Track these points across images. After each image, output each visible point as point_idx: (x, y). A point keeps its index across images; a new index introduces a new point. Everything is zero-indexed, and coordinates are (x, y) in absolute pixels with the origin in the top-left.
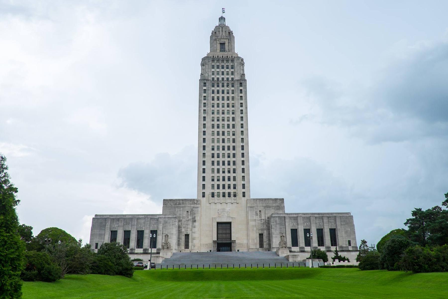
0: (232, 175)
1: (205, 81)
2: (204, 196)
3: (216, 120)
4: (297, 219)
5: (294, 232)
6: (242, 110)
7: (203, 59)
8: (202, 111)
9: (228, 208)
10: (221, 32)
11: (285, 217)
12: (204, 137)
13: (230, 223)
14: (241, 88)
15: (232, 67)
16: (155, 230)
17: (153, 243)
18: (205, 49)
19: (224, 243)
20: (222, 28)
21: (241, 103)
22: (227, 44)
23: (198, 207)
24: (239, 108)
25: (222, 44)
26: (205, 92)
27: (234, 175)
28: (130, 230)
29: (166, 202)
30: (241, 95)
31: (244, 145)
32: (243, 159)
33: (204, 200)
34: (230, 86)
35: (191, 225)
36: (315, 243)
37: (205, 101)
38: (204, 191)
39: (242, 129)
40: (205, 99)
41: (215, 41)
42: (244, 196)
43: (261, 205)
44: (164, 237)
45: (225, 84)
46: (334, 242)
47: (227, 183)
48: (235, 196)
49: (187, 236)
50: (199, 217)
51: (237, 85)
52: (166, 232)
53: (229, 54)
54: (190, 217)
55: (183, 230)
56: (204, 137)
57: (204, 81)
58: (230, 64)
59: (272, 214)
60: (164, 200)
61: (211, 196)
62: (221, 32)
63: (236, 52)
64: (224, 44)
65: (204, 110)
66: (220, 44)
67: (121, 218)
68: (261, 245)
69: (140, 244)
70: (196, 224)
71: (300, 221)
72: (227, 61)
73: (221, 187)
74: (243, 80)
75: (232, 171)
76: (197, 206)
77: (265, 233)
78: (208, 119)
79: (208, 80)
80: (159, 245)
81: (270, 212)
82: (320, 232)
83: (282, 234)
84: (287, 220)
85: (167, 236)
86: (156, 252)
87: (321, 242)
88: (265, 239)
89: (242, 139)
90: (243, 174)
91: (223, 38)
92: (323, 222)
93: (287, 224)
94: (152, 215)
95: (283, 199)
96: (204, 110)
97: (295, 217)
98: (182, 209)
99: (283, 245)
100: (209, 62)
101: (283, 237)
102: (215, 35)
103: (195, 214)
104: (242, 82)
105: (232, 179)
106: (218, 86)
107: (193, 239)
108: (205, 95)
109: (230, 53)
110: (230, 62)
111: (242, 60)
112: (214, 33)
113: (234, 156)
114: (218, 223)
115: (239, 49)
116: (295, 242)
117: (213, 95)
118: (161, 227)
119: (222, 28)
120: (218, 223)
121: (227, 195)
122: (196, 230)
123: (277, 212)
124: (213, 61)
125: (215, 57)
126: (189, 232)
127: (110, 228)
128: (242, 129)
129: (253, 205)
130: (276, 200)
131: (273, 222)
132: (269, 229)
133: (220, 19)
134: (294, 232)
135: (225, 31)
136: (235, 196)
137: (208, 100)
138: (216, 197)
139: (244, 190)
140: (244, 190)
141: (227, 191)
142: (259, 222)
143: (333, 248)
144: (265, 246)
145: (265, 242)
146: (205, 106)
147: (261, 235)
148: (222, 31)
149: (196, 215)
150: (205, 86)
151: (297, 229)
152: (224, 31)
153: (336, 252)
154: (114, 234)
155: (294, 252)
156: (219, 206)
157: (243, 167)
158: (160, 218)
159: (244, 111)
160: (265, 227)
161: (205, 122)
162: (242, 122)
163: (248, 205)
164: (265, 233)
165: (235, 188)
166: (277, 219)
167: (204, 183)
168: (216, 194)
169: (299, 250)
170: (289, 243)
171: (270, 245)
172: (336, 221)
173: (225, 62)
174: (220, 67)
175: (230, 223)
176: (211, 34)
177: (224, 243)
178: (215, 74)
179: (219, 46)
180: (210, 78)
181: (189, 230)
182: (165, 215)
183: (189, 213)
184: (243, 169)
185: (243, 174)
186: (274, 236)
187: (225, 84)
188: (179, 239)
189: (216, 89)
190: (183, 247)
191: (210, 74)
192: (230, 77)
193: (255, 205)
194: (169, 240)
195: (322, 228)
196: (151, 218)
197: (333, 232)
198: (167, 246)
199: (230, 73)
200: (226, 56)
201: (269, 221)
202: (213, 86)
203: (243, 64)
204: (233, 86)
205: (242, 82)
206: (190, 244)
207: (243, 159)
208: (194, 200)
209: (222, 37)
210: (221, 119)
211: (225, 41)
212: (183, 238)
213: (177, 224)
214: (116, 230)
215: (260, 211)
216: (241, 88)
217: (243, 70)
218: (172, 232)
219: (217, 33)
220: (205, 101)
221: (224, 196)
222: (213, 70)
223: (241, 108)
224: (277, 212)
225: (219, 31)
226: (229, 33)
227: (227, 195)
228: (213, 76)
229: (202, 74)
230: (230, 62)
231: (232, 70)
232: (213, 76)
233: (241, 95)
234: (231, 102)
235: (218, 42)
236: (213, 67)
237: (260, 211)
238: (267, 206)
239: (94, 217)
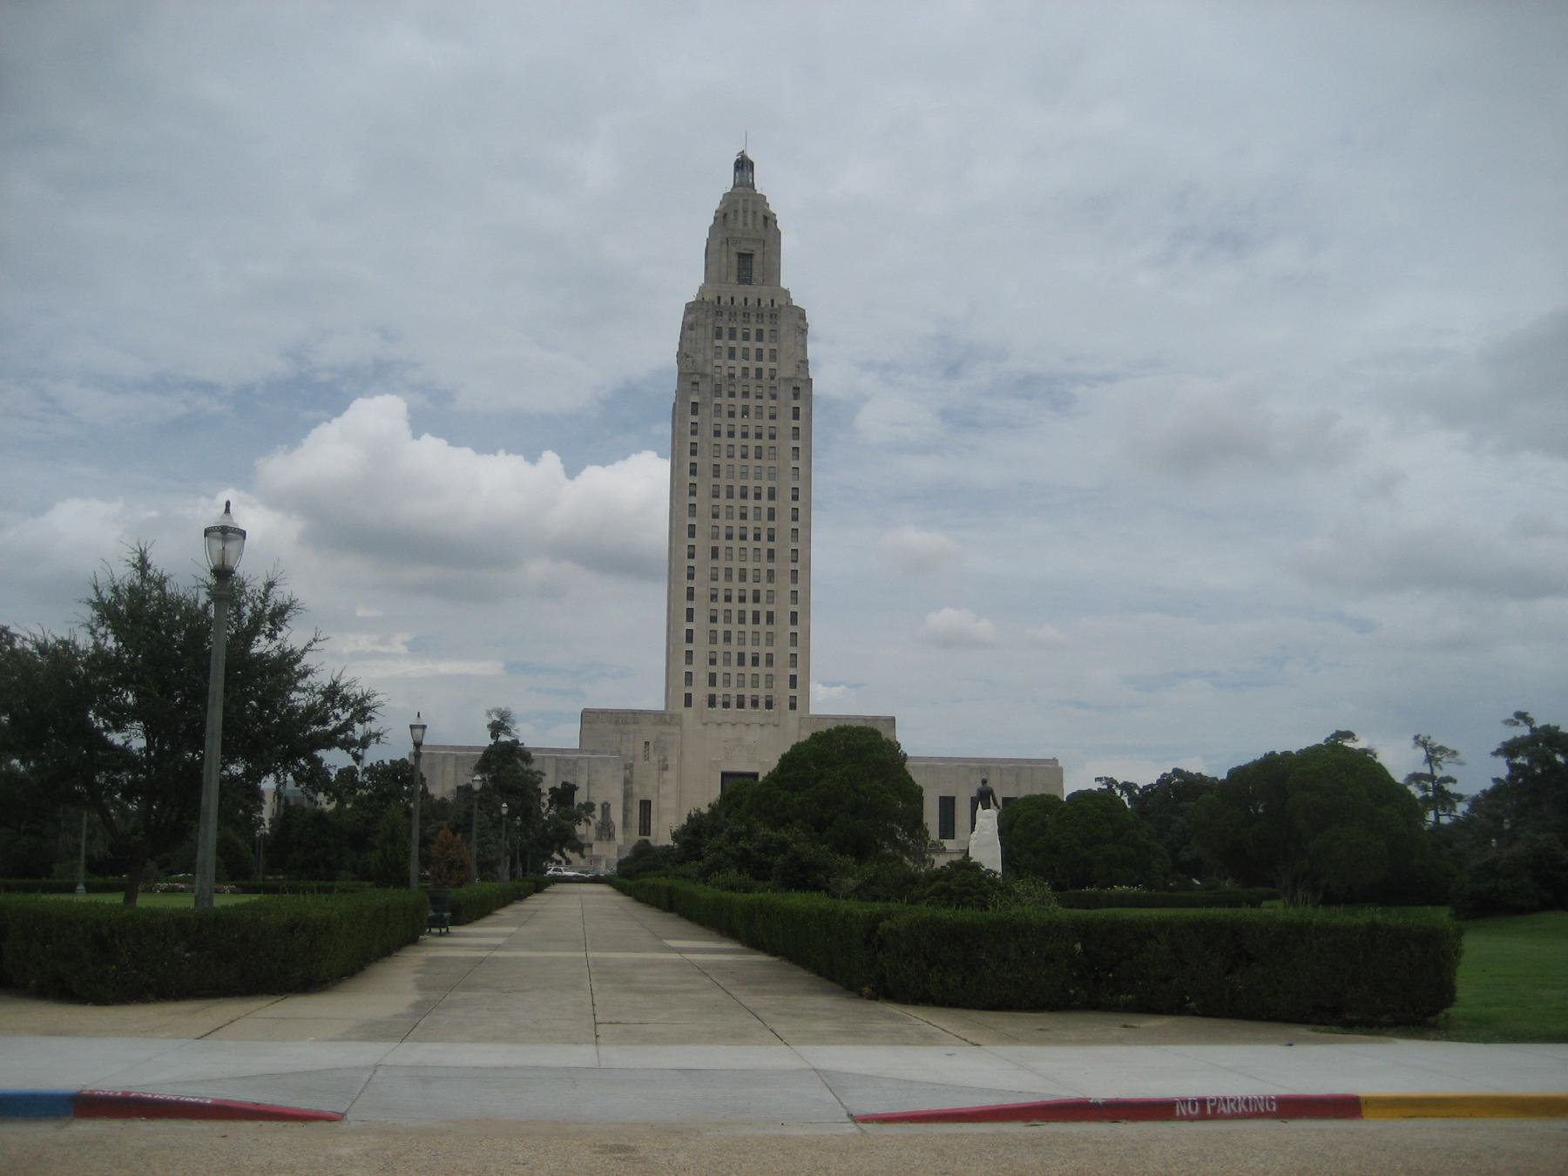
1: (697, 378)
2: (688, 700)
14: (796, 403)
20: (746, 201)
22: (757, 258)
25: (745, 258)
29: (590, 718)
33: (688, 714)
34: (766, 395)
39: (795, 525)
42: (793, 706)
48: (769, 705)
49: (646, 806)
51: (785, 393)
53: (765, 293)
55: (636, 789)
56: (692, 542)
61: (706, 704)
63: (784, 284)
64: (751, 255)
66: (740, 255)
70: (670, 775)
95: (893, 719)
104: (799, 384)
105: (762, 659)
108: (695, 419)
111: (802, 315)
112: (722, 217)
114: (725, 775)
120: (725, 775)
121: (748, 702)
126: (649, 795)
128: (795, 525)
136: (769, 705)
138: (719, 706)
139: (792, 692)
157: (792, 629)
174: (739, 335)
179: (734, 259)
188: (626, 811)
189: (724, 401)
191: (710, 354)
203: (804, 331)
219: (731, 216)
221: (741, 705)
222: (718, 343)
226: (766, 218)
228: (718, 362)
235: (734, 250)
236: (719, 335)
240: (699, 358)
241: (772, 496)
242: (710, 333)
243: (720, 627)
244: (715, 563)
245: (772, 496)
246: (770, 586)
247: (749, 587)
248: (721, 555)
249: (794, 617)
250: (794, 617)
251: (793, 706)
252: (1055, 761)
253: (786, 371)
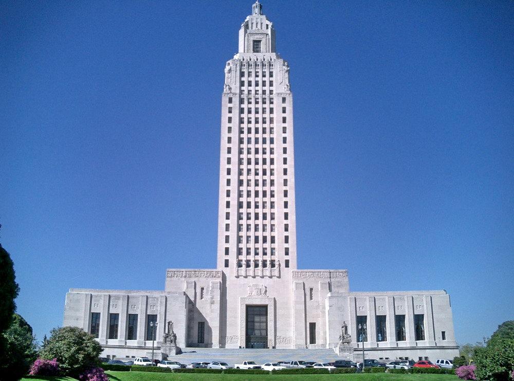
1: (231, 96)
13: (266, 307)
16: (155, 314)
19: (255, 337)
42: (287, 265)
44: (167, 324)
64: (260, 41)
90: (286, 234)
99: (345, 339)
121: (260, 264)
134: (361, 320)
135: (262, 23)
154: (95, 317)
157: (286, 222)
162: (285, 156)
168: (244, 263)
177: (255, 337)
188: (189, 329)
219: (250, 26)
227: (260, 264)
235: (252, 38)
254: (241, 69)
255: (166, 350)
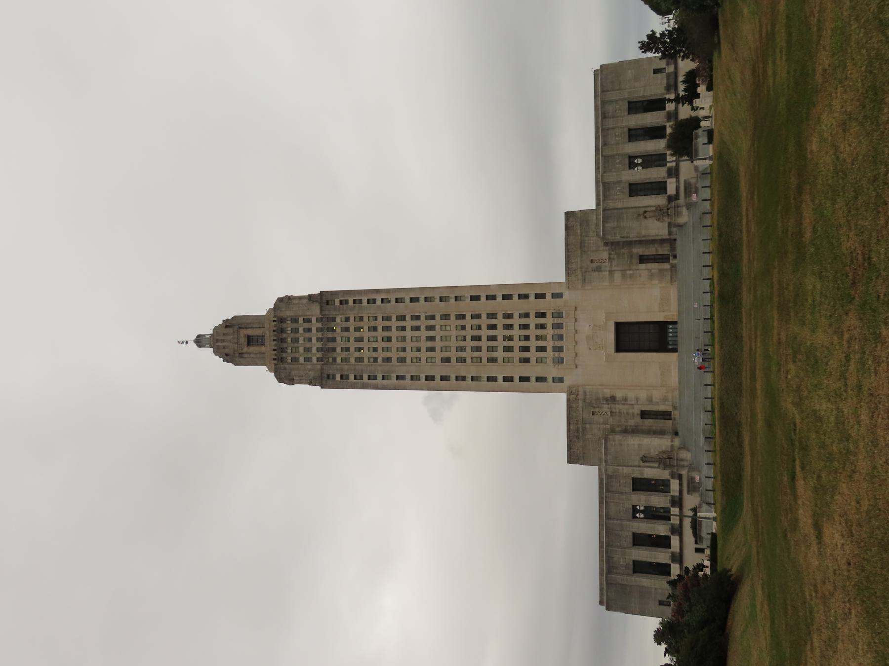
0: (516, 321)
2: (561, 380)
3: (403, 355)
4: (609, 183)
5: (635, 189)
6: (383, 301)
7: (280, 380)
8: (385, 382)
9: (585, 328)
10: (224, 344)
11: (604, 210)
12: (438, 378)
13: (618, 325)
15: (295, 320)
16: (631, 481)
17: (661, 486)
18: (260, 376)
20: (217, 341)
21: (368, 301)
22: (250, 332)
23: (585, 392)
24: (379, 306)
25: (250, 340)
26: (347, 377)
27: (516, 316)
28: (631, 534)
29: (573, 458)
30: (351, 303)
31: (453, 296)
32: (483, 299)
35: (621, 407)
36: (658, 145)
37: (365, 377)
38: (550, 380)
39: (422, 300)
40: (361, 378)
41: (245, 356)
43: (579, 260)
45: (330, 335)
46: (656, 105)
47: (533, 332)
49: (644, 415)
50: (605, 390)
52: (637, 461)
53: (269, 327)
54: (606, 408)
55: (632, 422)
57: (325, 380)
58: (289, 326)
59: (598, 235)
60: (569, 462)
62: (224, 344)
63: (264, 313)
65: (383, 378)
66: (249, 344)
67: (607, 552)
68: (664, 259)
69: (662, 542)
70: (619, 395)
71: (612, 177)
72: (283, 331)
73: (541, 343)
74: (321, 299)
75: (508, 321)
76: (581, 393)
77: (639, 250)
78: (402, 370)
79: (322, 369)
80: (665, 474)
81: (593, 240)
82: (634, 135)
83: (639, 215)
84: (611, 204)
85: (644, 459)
86: (677, 481)
87: (655, 132)
88: (651, 251)
89: (441, 299)
90: (516, 297)
91: (238, 339)
92: (613, 128)
93: (620, 205)
94: (601, 488)
95: (567, 214)
96: (383, 378)
97: (604, 188)
98: (588, 426)
99: (661, 213)
100: (285, 369)
101: (644, 214)
102: (233, 356)
103: (598, 399)
104: (324, 301)
105: (524, 321)
106: (334, 350)
107: (650, 400)
108: (352, 377)
109: (266, 325)
110: (284, 326)
111: (280, 300)
112: (228, 357)
113: (476, 316)
114: (619, 348)
115: (259, 305)
116: (659, 188)
117: (352, 360)
118: (626, 470)
119: (217, 341)
120: (619, 348)
122: (631, 395)
123: (593, 227)
124: (282, 360)
125: (276, 355)
126: (637, 410)
127: (629, 575)
128: (422, 300)
129: (580, 277)
130: (567, 228)
131: (615, 234)
132: (630, 244)
133: (199, 346)
134: (635, 189)
135: (224, 334)
136: (558, 314)
137: (362, 371)
138: (562, 355)
139: (549, 296)
140: (549, 296)
141: (549, 332)
142: (614, 263)
143: (670, 107)
144: (664, 250)
145: (657, 250)
146: (375, 378)
147: (643, 259)
148: (223, 341)
149: (601, 396)
150: (334, 377)
151: (630, 185)
152: (222, 338)
153: (677, 100)
154: (639, 567)
155: (678, 189)
156: (583, 347)
157: (499, 299)
158: (606, 471)
159: (384, 296)
160: (625, 251)
161: (408, 377)
162: (408, 301)
163: (580, 287)
164: (639, 250)
165: (543, 315)
166: (608, 225)
167: (533, 379)
169: (674, 180)
170: (658, 200)
171: (662, 241)
172: (611, 101)
173: (285, 335)
175: (618, 325)
176: (230, 364)
178: (309, 355)
179: (252, 349)
180: (319, 367)
181: (631, 411)
182: (600, 460)
183: (597, 410)
184: (504, 297)
185: (516, 297)
186: (644, 232)
187: (330, 335)
190: (669, 423)
192: (315, 325)
193: (579, 272)
194: (654, 453)
195: (626, 130)
196: (608, 491)
197: (635, 107)
198: (666, 460)
199: (307, 325)
200: (272, 333)
201: (612, 243)
202: (334, 360)
204: (334, 320)
205: (324, 299)
206: (662, 408)
207: (483, 299)
208: (568, 400)
209: (236, 341)
210: (401, 344)
211: (242, 335)
212: (648, 422)
213: (618, 437)
214: (631, 563)
215: (592, 261)
216: (337, 302)
217: (301, 298)
218: (636, 446)
219: (227, 351)
220: (365, 377)
222: (301, 360)
223: (379, 302)
224: (593, 227)
225: (224, 348)
226: (226, 327)
228: (314, 360)
229: (310, 384)
230: (284, 326)
231: (301, 320)
232: (314, 360)
233: (351, 303)
234: (365, 324)
235: (245, 349)
237: (592, 261)
238: (581, 247)
239: (604, 607)
240: (312, 374)
241: (403, 318)
242: (296, 366)
243: (500, 354)
244: (453, 360)
245: (403, 318)
246: (484, 316)
247: (484, 333)
248: (447, 355)
249: (525, 297)
250: (525, 297)
251: (557, 296)
252: (596, 73)
253: (315, 311)
254: (289, 364)
255: (683, 466)
